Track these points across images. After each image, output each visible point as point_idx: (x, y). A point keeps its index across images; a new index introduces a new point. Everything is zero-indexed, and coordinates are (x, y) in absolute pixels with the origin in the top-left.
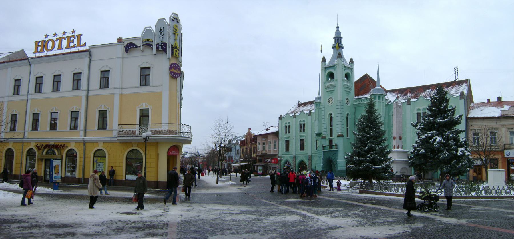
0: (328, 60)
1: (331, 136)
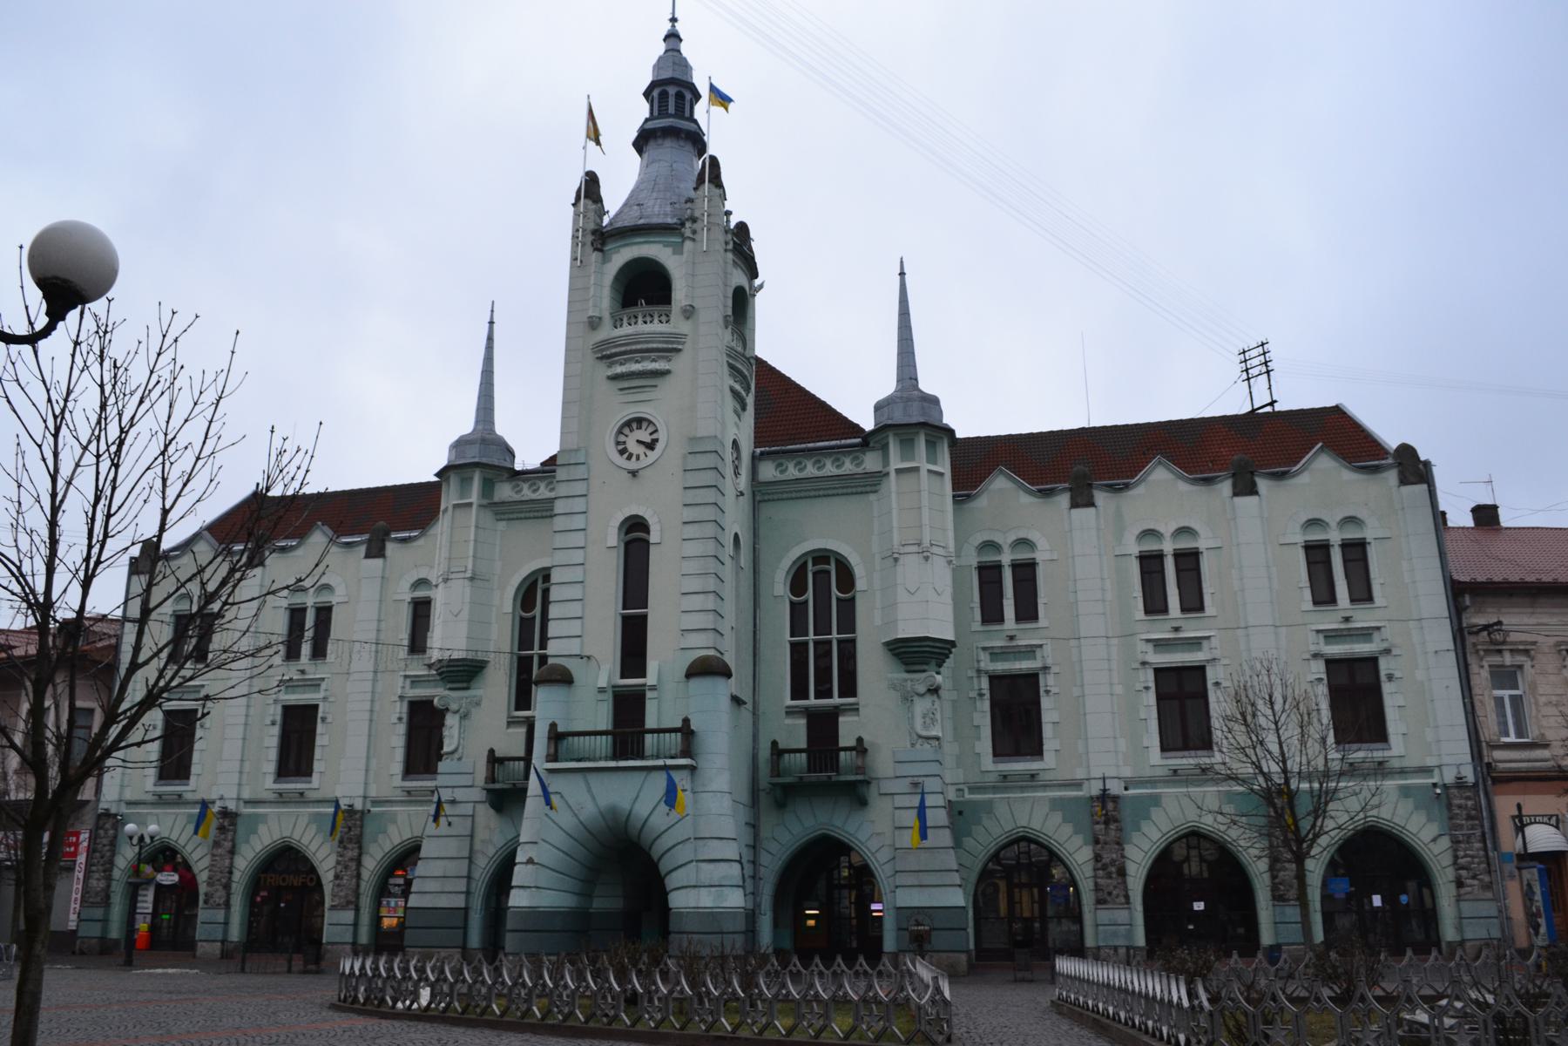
0: (614, 198)
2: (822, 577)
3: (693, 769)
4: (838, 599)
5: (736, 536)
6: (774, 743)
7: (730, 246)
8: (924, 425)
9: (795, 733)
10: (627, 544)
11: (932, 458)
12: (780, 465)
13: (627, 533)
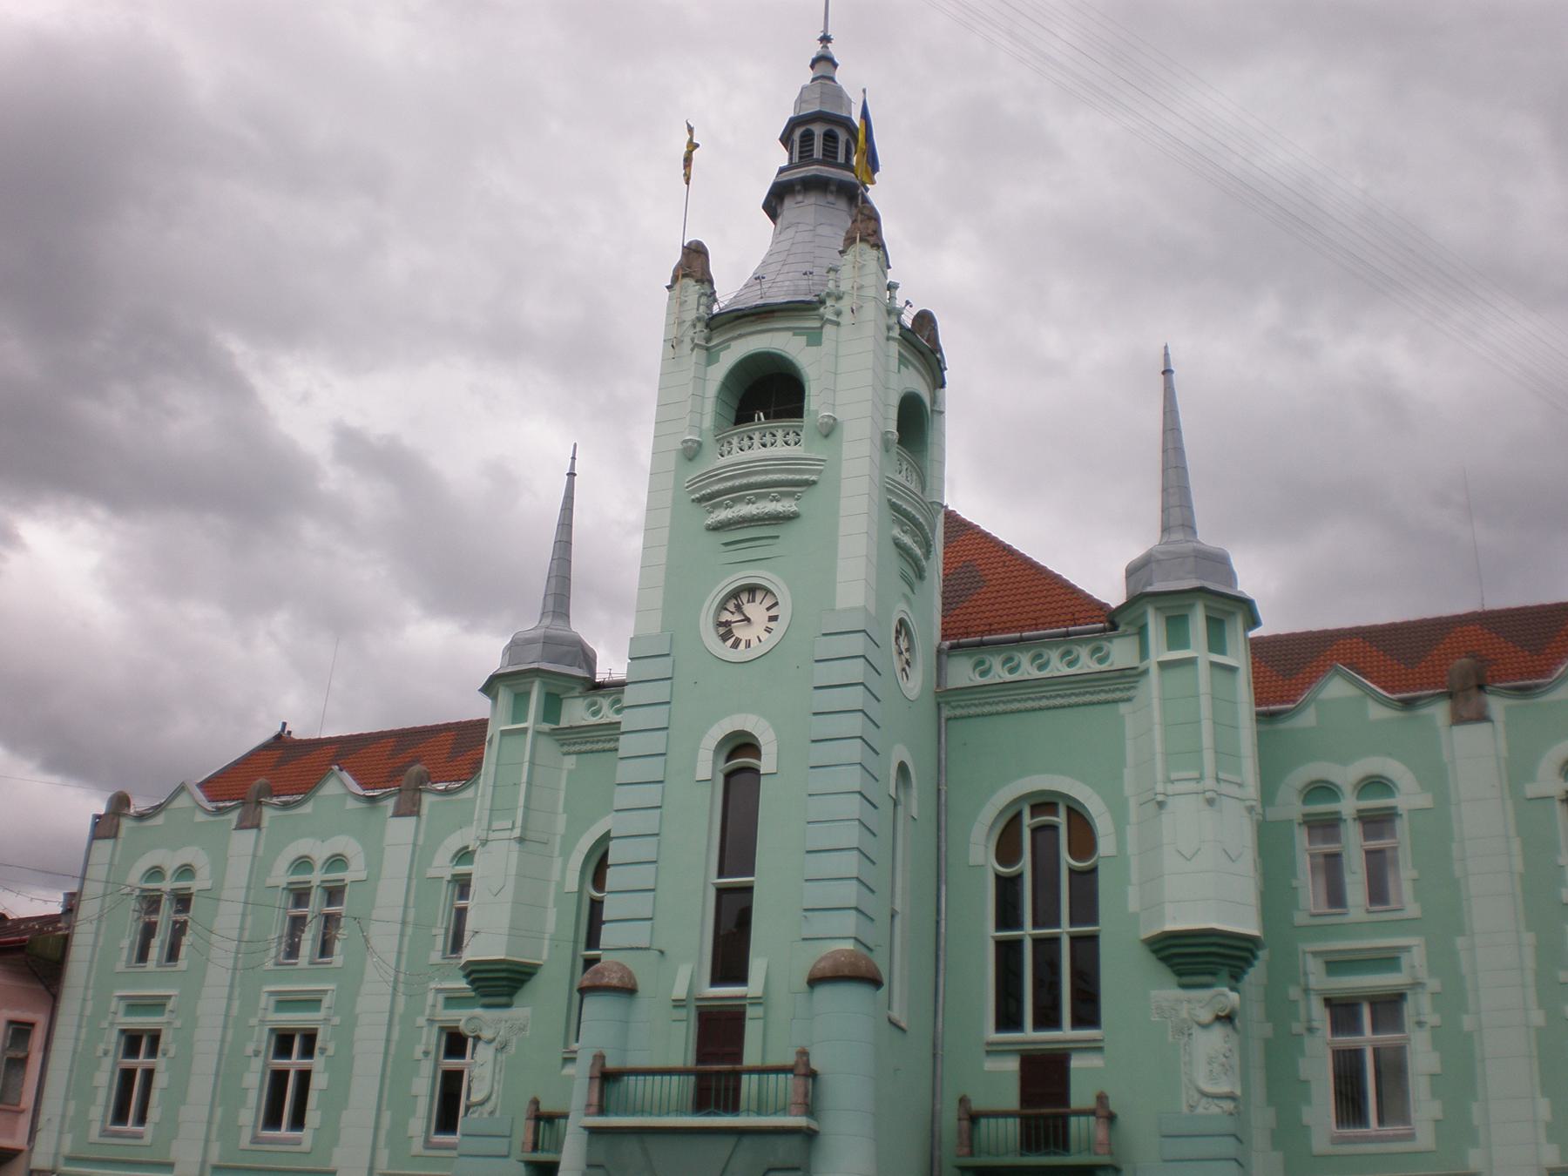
1: (730, 959)
2: (1045, 833)
3: (809, 1135)
4: (1072, 871)
5: (903, 769)
6: (963, 1101)
7: (896, 333)
8: (1201, 591)
9: (998, 1081)
10: (729, 776)
11: (1216, 642)
12: (981, 663)
13: (729, 758)
